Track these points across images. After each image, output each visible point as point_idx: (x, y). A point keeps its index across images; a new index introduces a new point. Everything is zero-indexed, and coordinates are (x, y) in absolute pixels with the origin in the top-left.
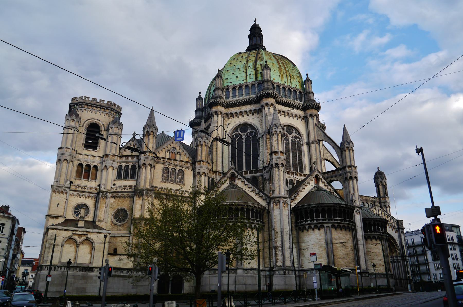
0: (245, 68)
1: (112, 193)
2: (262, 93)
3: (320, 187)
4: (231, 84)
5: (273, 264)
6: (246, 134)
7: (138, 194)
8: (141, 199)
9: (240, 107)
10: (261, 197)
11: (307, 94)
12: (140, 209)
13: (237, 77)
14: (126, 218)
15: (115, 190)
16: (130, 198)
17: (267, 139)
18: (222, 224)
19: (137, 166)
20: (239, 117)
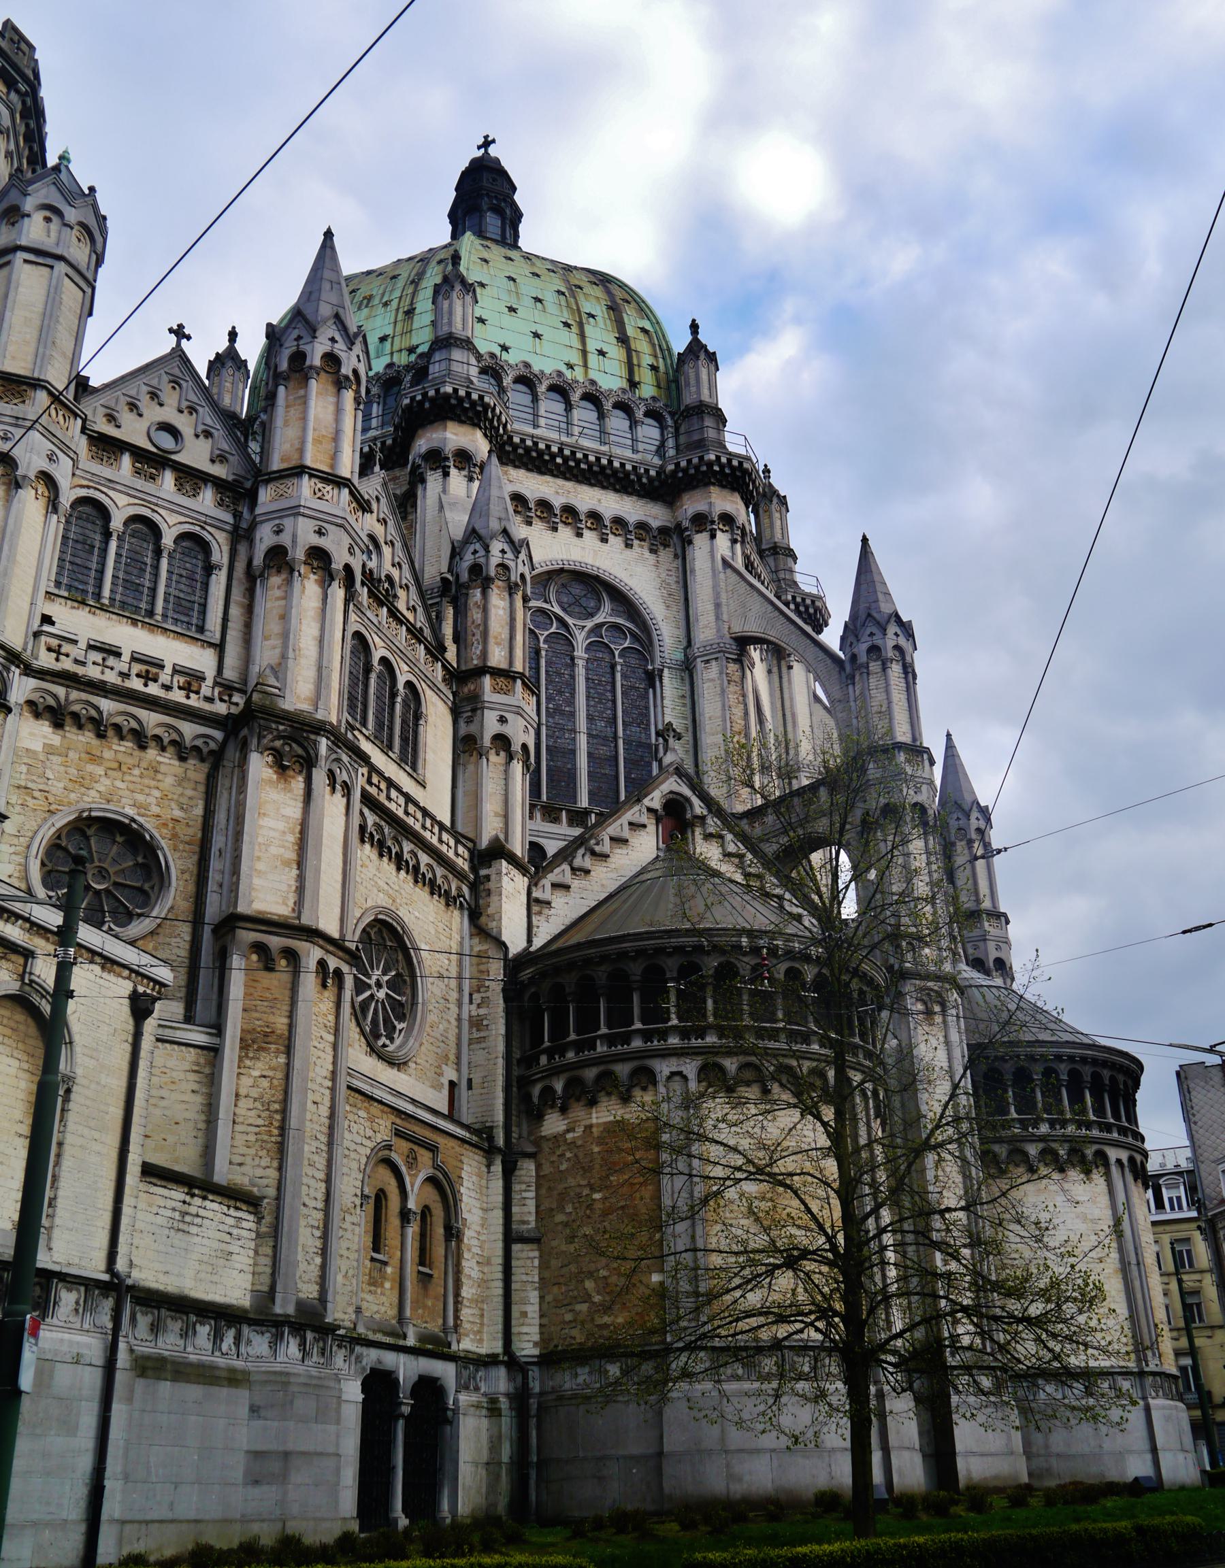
0: (573, 314)
1: (42, 674)
2: (713, 457)
4: (505, 356)
6: (589, 624)
7: (278, 743)
9: (569, 485)
11: (777, 553)
12: (293, 856)
13: (537, 335)
14: (145, 898)
15: (67, 665)
16: (182, 759)
19: (220, 554)
20: (555, 529)
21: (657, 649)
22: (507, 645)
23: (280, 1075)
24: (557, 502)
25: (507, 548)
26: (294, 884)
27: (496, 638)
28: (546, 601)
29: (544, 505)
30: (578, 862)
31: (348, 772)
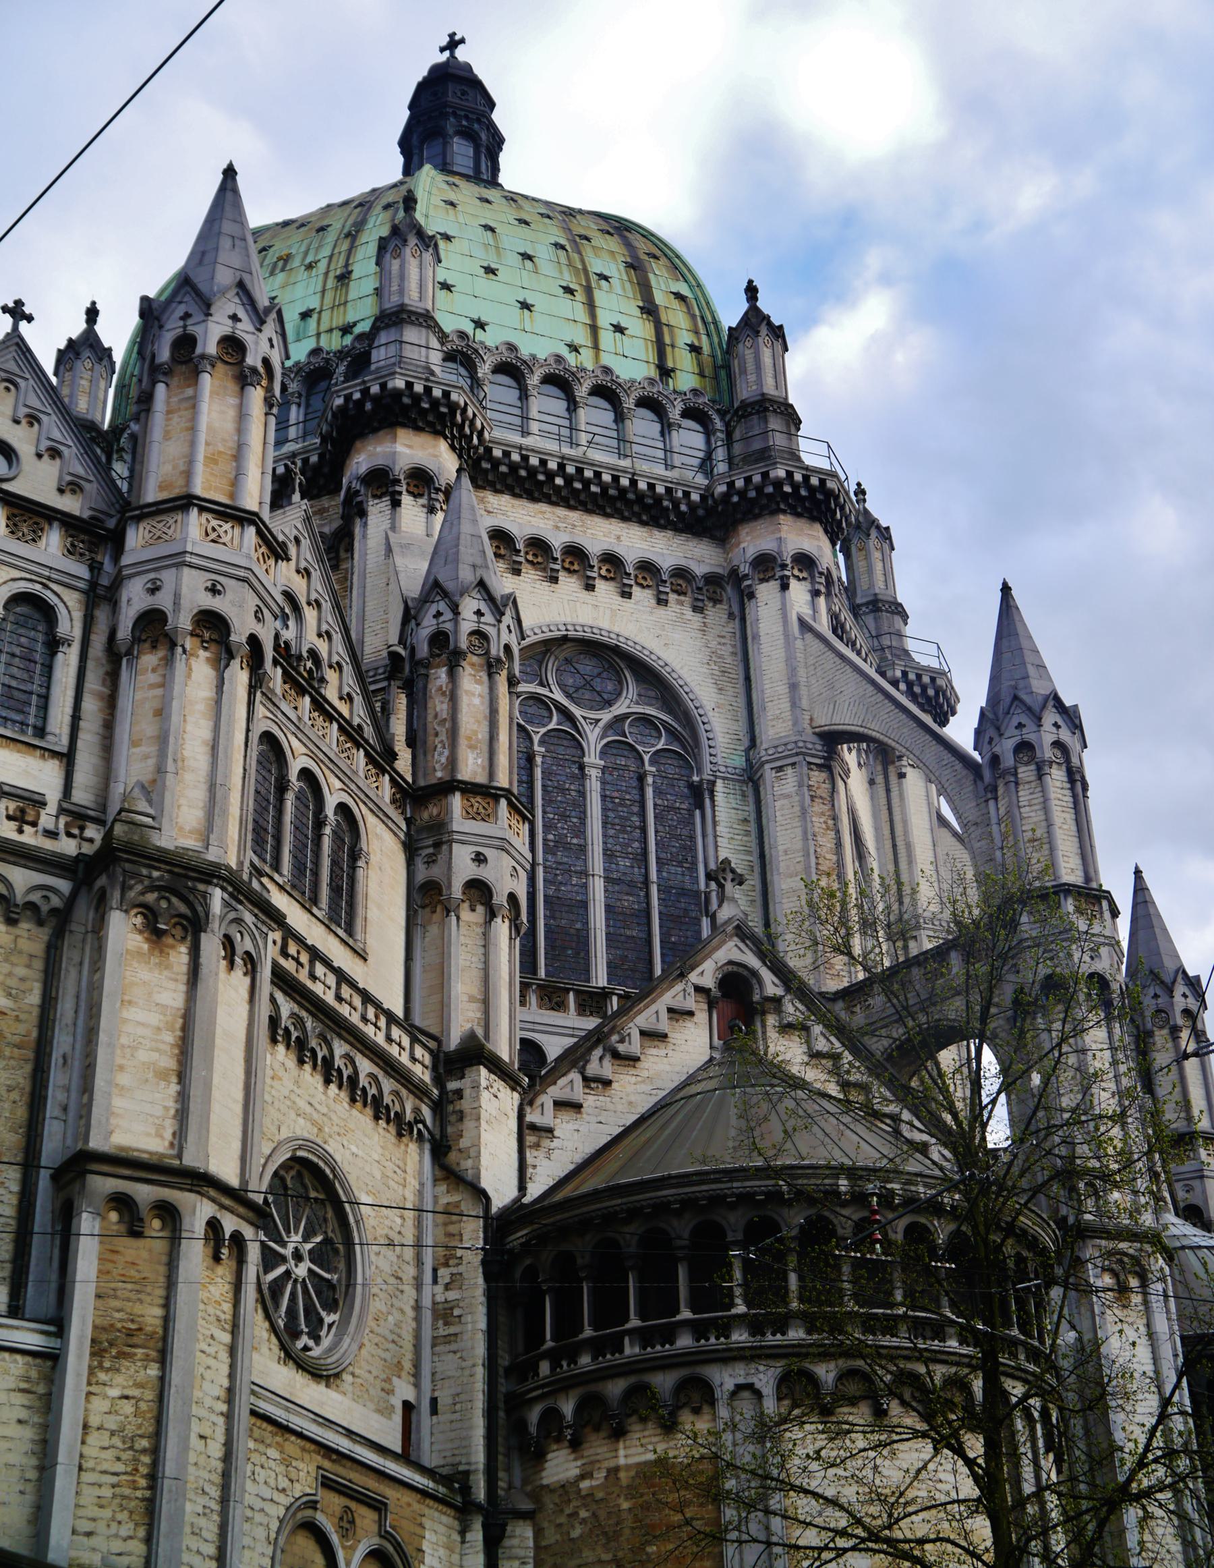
2: (781, 473)
6: (606, 716)
7: (151, 898)
9: (574, 516)
11: (878, 610)
12: (170, 1063)
13: (525, 306)
17: (812, 798)
19: (70, 624)
20: (554, 580)
21: (706, 751)
22: (485, 748)
23: (149, 1395)
24: (558, 541)
25: (484, 607)
26: (172, 1105)
27: (469, 738)
28: (541, 684)
29: (538, 545)
30: (593, 1068)
31: (253, 939)
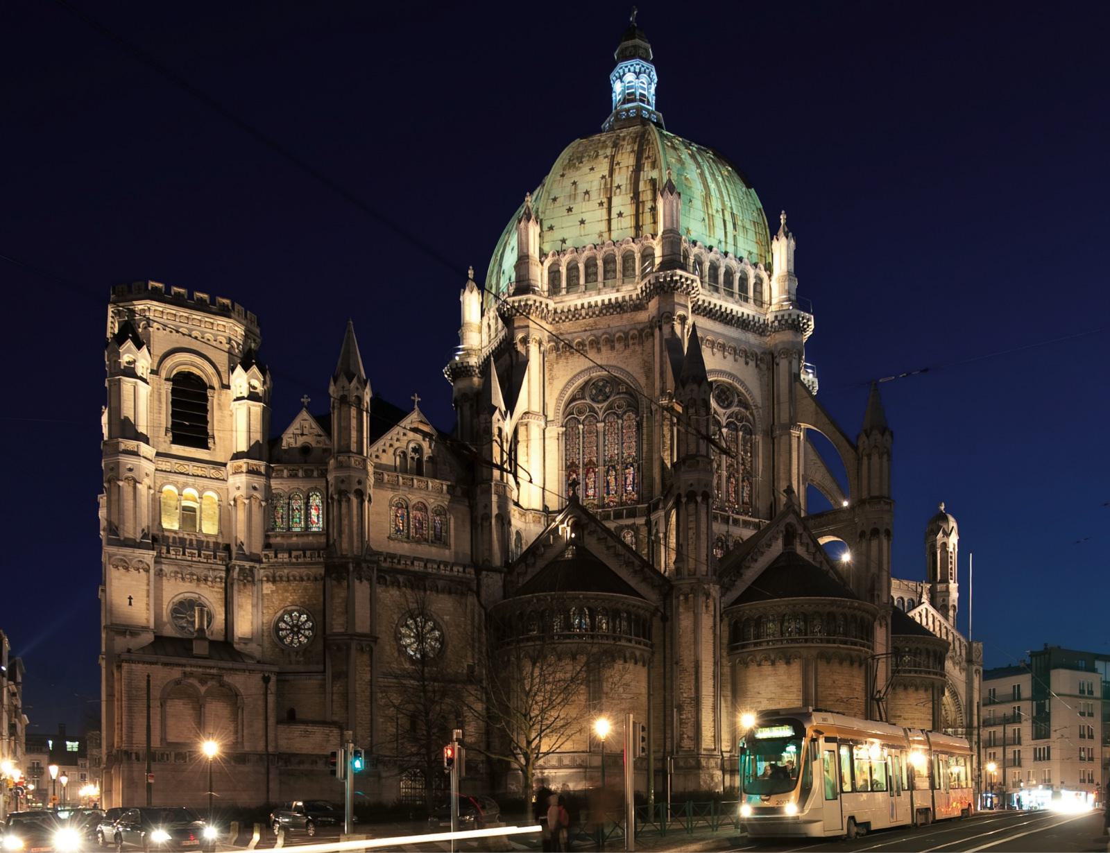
0: (607, 191)
3: (798, 555)
5: (672, 744)
8: (345, 583)
10: (644, 580)
13: (582, 222)
18: (554, 648)
